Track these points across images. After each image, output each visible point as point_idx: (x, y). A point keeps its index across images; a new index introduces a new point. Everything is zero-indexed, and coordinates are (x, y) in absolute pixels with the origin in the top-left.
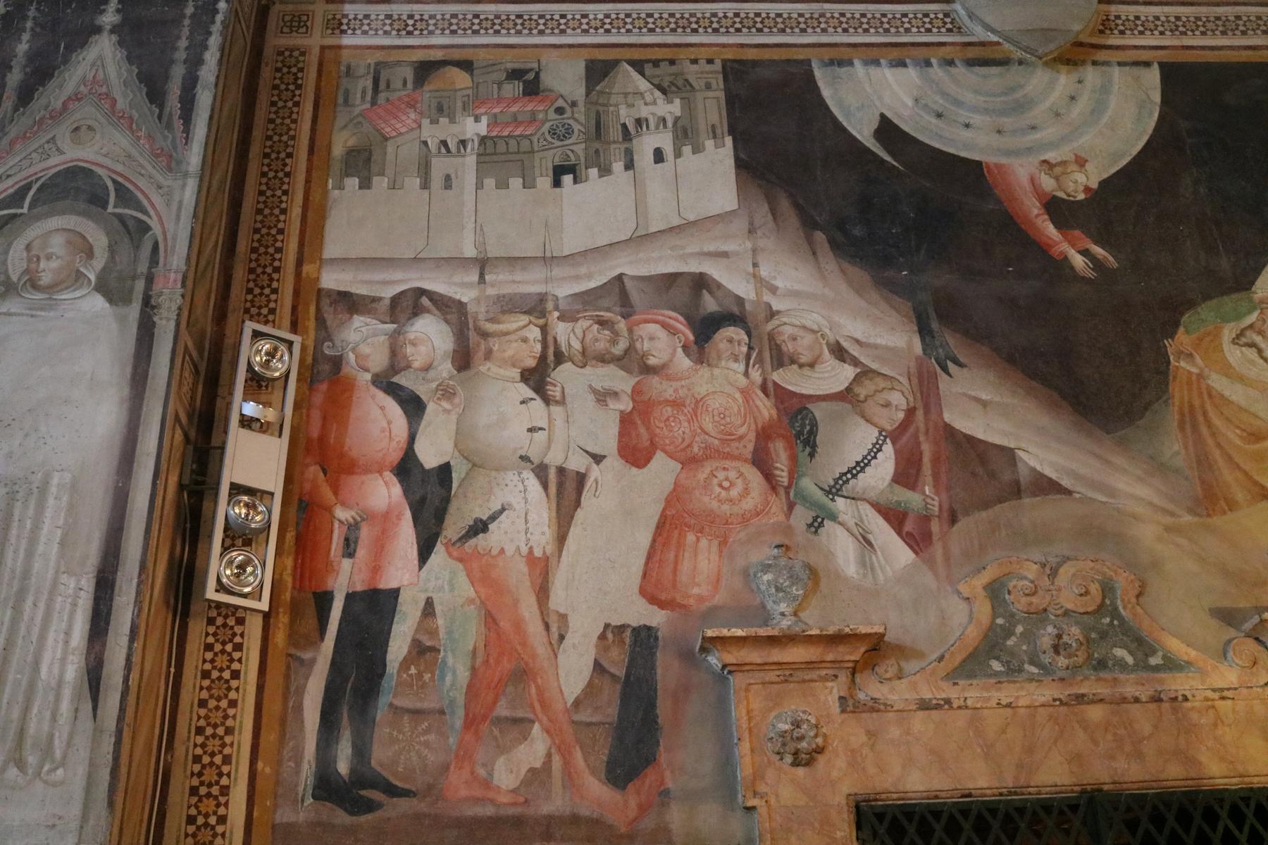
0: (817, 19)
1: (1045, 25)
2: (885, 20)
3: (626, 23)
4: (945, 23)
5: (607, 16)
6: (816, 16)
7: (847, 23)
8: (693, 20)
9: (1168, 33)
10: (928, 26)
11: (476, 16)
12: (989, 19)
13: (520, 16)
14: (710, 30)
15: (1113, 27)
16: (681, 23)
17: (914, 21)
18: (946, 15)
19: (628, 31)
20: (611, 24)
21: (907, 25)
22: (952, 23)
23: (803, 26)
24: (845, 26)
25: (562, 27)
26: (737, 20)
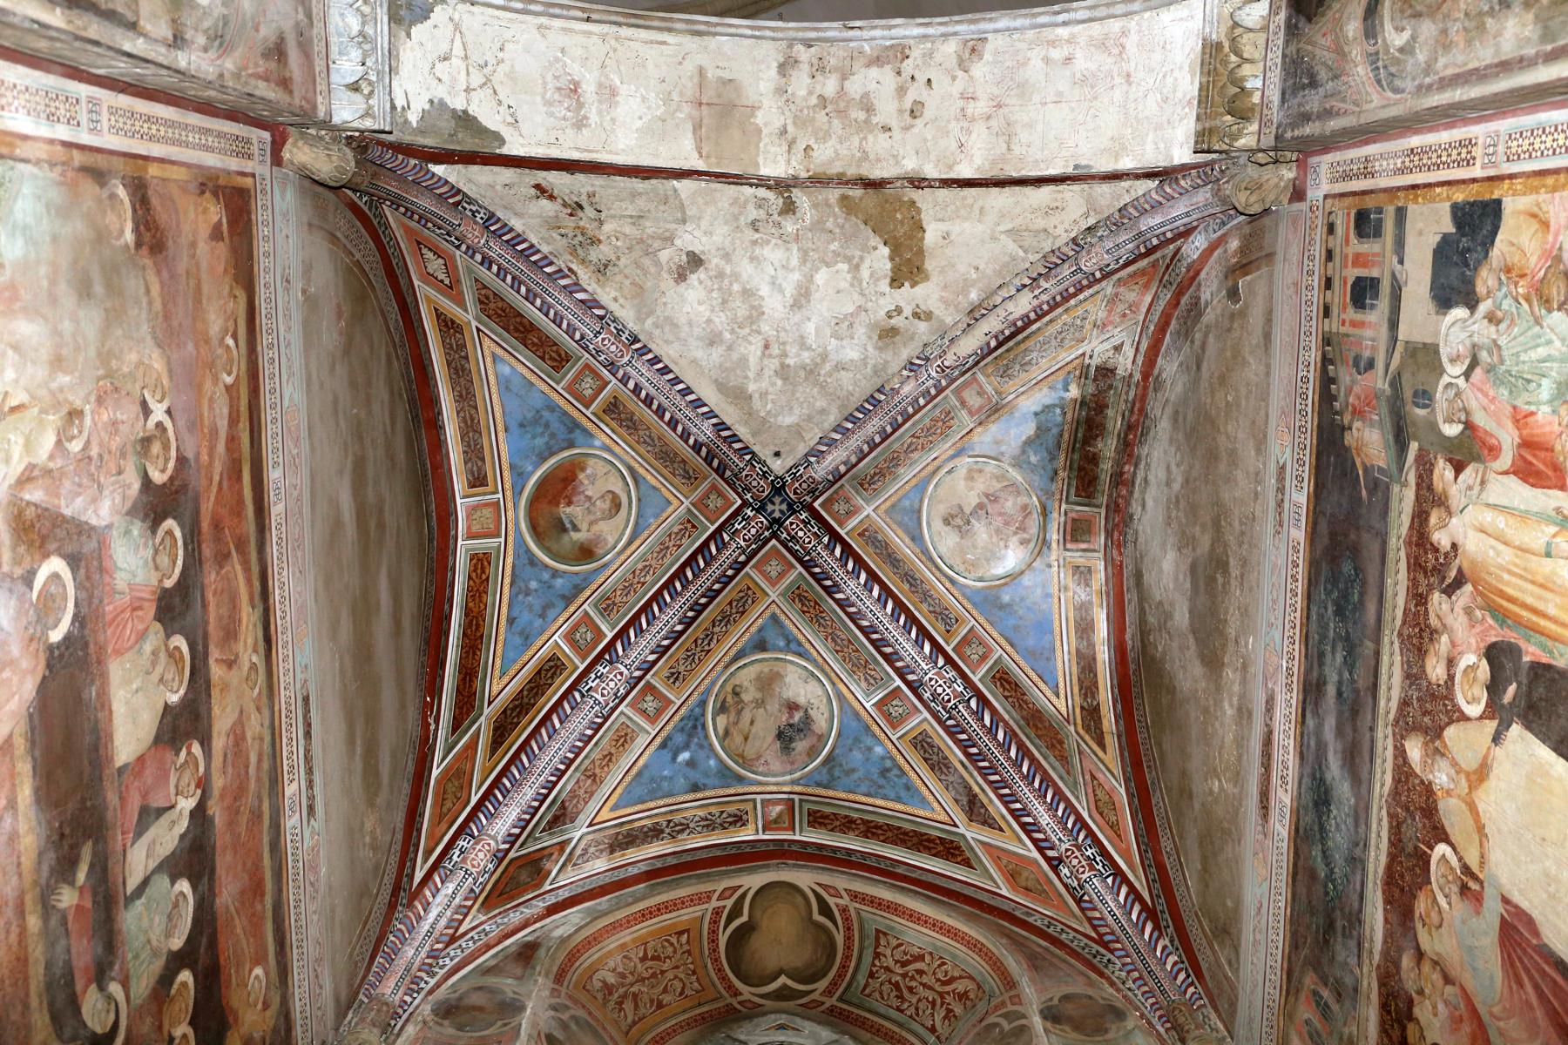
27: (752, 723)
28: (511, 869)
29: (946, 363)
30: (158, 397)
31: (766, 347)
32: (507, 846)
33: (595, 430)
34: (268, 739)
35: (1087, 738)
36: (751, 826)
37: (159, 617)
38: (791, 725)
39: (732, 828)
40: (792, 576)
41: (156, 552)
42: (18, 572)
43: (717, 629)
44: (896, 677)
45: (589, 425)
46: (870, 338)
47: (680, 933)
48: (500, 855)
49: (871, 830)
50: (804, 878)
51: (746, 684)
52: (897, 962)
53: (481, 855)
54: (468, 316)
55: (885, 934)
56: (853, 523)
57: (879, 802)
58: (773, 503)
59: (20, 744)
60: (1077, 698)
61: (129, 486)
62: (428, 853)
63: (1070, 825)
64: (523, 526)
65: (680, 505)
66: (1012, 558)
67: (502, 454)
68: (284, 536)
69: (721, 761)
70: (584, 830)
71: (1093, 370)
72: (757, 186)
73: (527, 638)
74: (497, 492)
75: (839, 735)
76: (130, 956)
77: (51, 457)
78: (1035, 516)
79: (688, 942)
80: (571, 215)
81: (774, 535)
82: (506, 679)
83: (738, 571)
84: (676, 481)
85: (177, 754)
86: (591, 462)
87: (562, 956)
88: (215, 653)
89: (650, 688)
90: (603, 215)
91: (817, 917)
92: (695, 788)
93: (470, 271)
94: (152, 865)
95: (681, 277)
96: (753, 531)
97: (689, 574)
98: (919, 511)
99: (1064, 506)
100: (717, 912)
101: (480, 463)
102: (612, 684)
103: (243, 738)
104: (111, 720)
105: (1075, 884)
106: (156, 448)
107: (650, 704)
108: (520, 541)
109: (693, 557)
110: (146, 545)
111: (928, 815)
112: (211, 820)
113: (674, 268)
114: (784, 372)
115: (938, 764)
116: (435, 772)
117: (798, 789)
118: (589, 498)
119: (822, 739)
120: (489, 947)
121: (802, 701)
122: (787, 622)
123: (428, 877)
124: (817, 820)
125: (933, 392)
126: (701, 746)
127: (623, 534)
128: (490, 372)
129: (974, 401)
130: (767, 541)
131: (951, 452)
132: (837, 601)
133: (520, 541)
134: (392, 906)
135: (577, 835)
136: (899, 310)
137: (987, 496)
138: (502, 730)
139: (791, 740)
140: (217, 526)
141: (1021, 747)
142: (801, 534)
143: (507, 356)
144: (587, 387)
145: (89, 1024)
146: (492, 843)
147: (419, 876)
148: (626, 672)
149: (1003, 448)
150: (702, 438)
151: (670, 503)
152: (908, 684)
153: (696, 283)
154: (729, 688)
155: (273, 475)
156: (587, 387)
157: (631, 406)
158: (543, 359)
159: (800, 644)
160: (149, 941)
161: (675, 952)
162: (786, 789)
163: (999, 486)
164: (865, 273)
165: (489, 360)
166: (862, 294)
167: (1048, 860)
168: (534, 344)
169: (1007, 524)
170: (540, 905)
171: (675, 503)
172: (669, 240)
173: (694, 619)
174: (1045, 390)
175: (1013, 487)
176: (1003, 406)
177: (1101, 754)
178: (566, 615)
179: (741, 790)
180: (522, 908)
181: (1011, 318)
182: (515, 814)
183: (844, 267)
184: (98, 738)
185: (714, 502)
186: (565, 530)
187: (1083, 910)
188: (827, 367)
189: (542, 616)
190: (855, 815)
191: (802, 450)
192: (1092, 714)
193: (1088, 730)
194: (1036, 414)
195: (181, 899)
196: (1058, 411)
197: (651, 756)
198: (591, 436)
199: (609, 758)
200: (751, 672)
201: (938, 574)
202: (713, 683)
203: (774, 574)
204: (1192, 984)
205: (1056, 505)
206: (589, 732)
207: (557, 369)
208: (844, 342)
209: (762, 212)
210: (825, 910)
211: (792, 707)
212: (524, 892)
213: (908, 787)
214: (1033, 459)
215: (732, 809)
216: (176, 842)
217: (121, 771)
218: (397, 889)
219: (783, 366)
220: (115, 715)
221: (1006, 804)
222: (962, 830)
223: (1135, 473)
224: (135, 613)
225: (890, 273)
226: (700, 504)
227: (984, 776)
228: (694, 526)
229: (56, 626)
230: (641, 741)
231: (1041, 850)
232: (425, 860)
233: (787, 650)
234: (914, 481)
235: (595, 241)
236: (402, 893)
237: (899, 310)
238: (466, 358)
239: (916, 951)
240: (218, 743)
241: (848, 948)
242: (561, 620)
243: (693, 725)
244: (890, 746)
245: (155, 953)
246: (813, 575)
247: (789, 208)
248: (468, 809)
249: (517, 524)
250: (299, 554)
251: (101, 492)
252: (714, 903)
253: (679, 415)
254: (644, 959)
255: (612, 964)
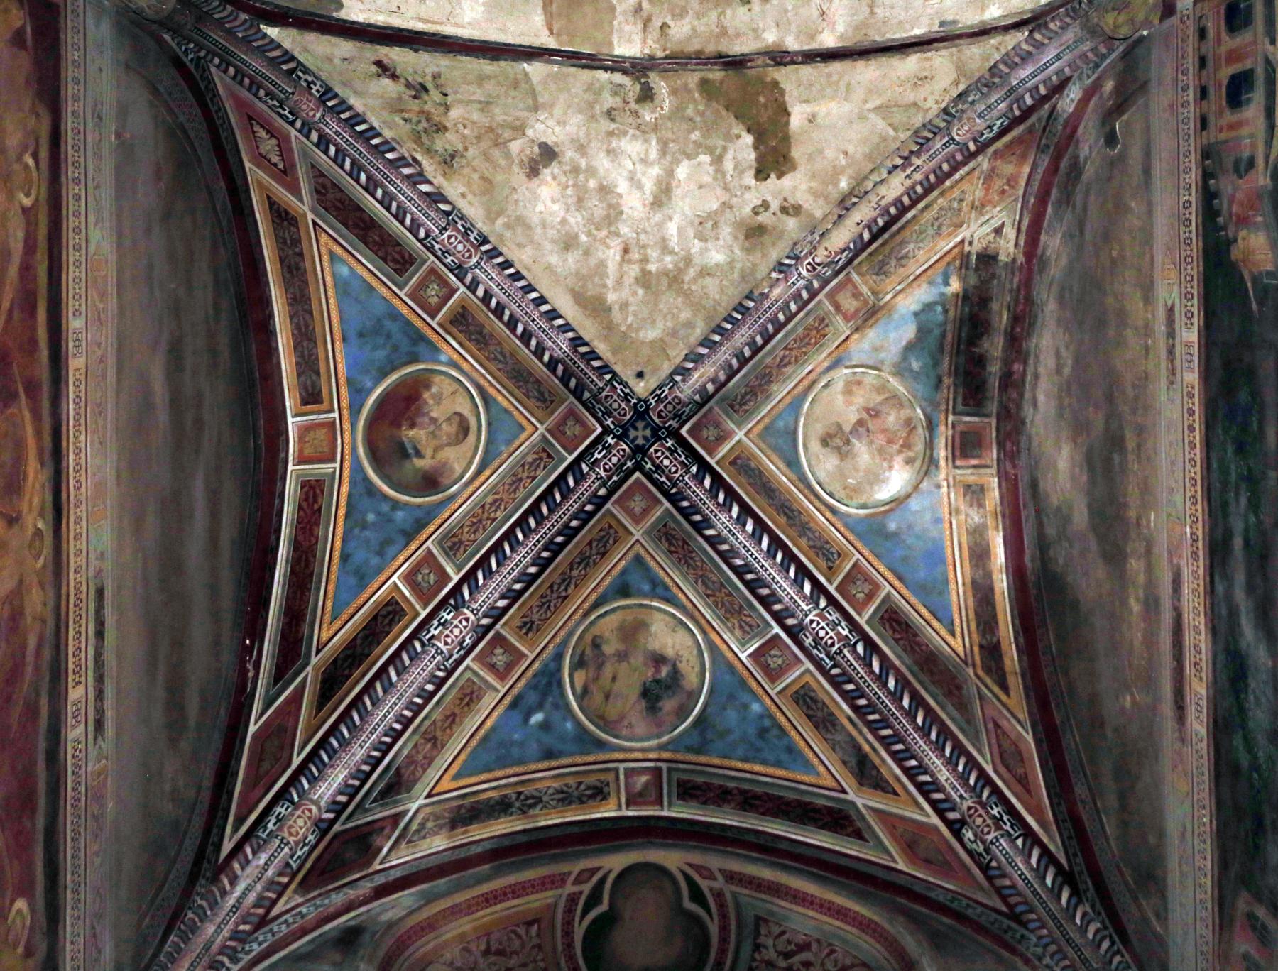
27: (614, 679)
28: (336, 844)
29: (818, 260)
31: (626, 251)
32: (331, 816)
33: (441, 345)
35: (989, 681)
36: (612, 801)
38: (657, 681)
39: (591, 803)
40: (658, 512)
43: (575, 573)
44: (773, 623)
45: (435, 338)
46: (736, 238)
47: (529, 924)
48: (323, 825)
49: (750, 800)
50: (672, 859)
51: (607, 634)
52: (779, 953)
53: (300, 822)
54: (304, 206)
55: (766, 921)
56: (724, 450)
57: (757, 768)
58: (636, 429)
60: (975, 636)
62: (240, 821)
63: (972, 782)
64: (361, 451)
65: (535, 430)
66: (897, 480)
67: (340, 367)
69: (578, 723)
70: (421, 801)
71: (974, 258)
72: (612, 70)
73: (362, 578)
74: (332, 411)
75: (712, 691)
78: (920, 431)
79: (538, 935)
80: (415, 97)
81: (638, 467)
82: (338, 624)
83: (599, 507)
84: (529, 403)
86: (437, 379)
87: (389, 941)
89: (499, 640)
90: (449, 98)
91: (688, 904)
92: (549, 755)
93: (305, 154)
95: (533, 171)
96: (615, 460)
97: (545, 510)
98: (795, 432)
99: (951, 418)
100: (573, 899)
101: (314, 377)
102: (456, 632)
105: (981, 849)
107: (500, 658)
108: (357, 468)
109: (549, 491)
111: (812, 780)
113: (525, 159)
114: (645, 280)
115: (823, 721)
116: (252, 728)
117: (666, 755)
118: (434, 420)
119: (694, 695)
120: (304, 932)
121: (670, 653)
122: (652, 564)
123: (238, 848)
124: (687, 791)
125: (805, 295)
126: (556, 706)
127: (470, 463)
128: (327, 271)
129: (849, 304)
130: (630, 473)
131: (826, 364)
132: (707, 538)
133: (357, 468)
134: (193, 877)
135: (414, 807)
136: (765, 205)
137: (867, 410)
138: (331, 682)
139: (658, 698)
141: (915, 696)
142: (666, 462)
143: (345, 255)
144: (433, 292)
146: (314, 808)
147: (227, 847)
148: (472, 618)
149: (883, 355)
150: (558, 353)
151: (523, 429)
152: (787, 629)
153: (549, 178)
154: (588, 638)
156: (433, 292)
157: (480, 317)
158: (384, 260)
159: (667, 588)
161: (523, 945)
162: (652, 755)
163: (879, 399)
164: (728, 165)
165: (326, 258)
166: (726, 188)
167: (949, 823)
168: (376, 243)
169: (890, 441)
170: (366, 887)
171: (529, 429)
172: (520, 129)
173: (549, 561)
174: (925, 286)
175: (894, 400)
176: (882, 308)
177: (1004, 697)
178: (406, 553)
179: (601, 757)
180: (345, 890)
181: (883, 203)
182: (341, 776)
183: (705, 158)
185: (572, 429)
186: (406, 456)
187: (990, 879)
188: (692, 272)
189: (381, 553)
190: (731, 785)
191: (666, 369)
192: (992, 652)
193: (988, 670)
194: (916, 314)
196: (939, 309)
197: (501, 717)
198: (436, 350)
199: (452, 719)
200: (612, 621)
201: (817, 503)
202: (571, 634)
203: (638, 510)
204: (1118, 952)
205: (943, 416)
206: (430, 687)
207: (400, 272)
208: (709, 245)
209: (618, 99)
210: (697, 895)
211: (658, 660)
212: (352, 870)
213: (791, 749)
214: (915, 365)
215: (591, 780)
219: (645, 273)
221: (899, 762)
222: (851, 796)
223: (1024, 370)
225: (754, 164)
226: (556, 431)
227: (874, 731)
228: (549, 456)
230: (489, 700)
231: (941, 813)
232: (236, 829)
233: (653, 595)
234: (787, 400)
235: (440, 129)
236: (205, 865)
237: (765, 205)
238: (301, 255)
239: (800, 939)
241: (724, 940)
242: (401, 558)
243: (547, 682)
244: (768, 702)
246: (681, 510)
247: (647, 95)
248: (289, 772)
249: (354, 449)
252: (570, 888)
253: (533, 327)
254: (487, 952)
255: (448, 956)
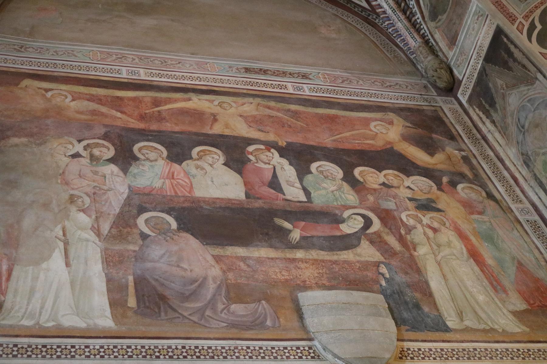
0: (233, 350)
1: (370, 355)
2: (274, 351)
3: (114, 352)
4: (310, 353)
5: (102, 347)
6: (232, 348)
7: (251, 353)
8: (157, 350)
9: (438, 358)
10: (300, 355)
11: (15, 346)
12: (336, 351)
13: (44, 346)
14: (167, 357)
15: (407, 355)
16: (149, 352)
17: (291, 352)
18: (310, 348)
19: (116, 357)
20: (104, 352)
21: (287, 354)
22: (314, 353)
23: (224, 354)
24: (250, 354)
25: (73, 354)
26: (184, 350)
30: (70, 146)
34: (258, 100)
37: (180, 162)
41: (148, 159)
42: (140, 242)
59: (218, 251)
61: (112, 172)
68: (157, 72)
76: (335, 203)
77: (90, 216)
85: (250, 160)
88: (207, 130)
94: (298, 185)
103: (254, 117)
104: (222, 199)
106: (96, 152)
110: (143, 165)
112: (289, 144)
140: (142, 118)
145: (356, 230)
155: (124, 75)
160: (333, 192)
184: (228, 208)
195: (320, 169)
216: (292, 168)
217: (247, 196)
218: (366, 20)
220: (220, 197)
224: (175, 177)
229: (170, 224)
240: (253, 134)
245: (340, 189)
250: (169, 62)
251: (112, 189)
